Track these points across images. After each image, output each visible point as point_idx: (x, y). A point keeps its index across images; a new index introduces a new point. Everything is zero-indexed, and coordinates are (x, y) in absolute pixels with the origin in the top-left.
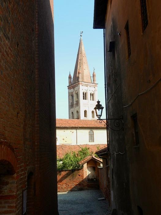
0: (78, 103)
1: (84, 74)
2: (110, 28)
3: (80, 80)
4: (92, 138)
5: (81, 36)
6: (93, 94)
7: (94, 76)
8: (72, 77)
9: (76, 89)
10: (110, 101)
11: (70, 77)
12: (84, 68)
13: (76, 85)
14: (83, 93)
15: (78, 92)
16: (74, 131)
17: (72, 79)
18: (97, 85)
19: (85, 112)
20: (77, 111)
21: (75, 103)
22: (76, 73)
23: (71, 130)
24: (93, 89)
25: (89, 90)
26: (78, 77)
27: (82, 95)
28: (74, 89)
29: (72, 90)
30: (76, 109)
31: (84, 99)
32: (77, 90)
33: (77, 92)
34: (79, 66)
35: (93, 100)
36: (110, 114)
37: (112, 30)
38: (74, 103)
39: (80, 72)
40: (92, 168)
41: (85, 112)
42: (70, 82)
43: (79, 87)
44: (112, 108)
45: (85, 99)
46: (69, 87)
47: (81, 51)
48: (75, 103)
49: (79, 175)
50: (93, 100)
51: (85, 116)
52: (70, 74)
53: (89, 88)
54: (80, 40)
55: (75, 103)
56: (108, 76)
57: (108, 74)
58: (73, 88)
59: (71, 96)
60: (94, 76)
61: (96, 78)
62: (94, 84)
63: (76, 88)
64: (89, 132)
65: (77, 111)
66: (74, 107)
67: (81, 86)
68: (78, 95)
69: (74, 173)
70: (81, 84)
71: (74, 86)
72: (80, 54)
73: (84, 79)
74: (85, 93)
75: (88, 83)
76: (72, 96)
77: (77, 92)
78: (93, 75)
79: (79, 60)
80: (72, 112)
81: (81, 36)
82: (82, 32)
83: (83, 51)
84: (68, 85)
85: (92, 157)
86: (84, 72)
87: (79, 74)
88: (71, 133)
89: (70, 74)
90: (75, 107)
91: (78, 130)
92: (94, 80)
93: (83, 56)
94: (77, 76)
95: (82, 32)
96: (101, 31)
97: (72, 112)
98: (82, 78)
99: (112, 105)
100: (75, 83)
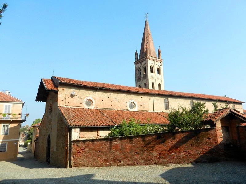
0: (146, 76)
1: (151, 50)
3: (148, 54)
4: (167, 106)
5: (146, 17)
7: (159, 52)
8: (139, 54)
9: (143, 63)
11: (136, 54)
12: (151, 45)
13: (143, 60)
14: (151, 67)
15: (145, 66)
16: (151, 98)
17: (138, 56)
18: (162, 60)
19: (153, 84)
20: (145, 84)
21: (142, 76)
22: (143, 49)
23: (148, 97)
24: (159, 64)
25: (157, 64)
26: (146, 53)
27: (150, 69)
28: (141, 64)
29: (139, 65)
30: (144, 81)
31: (151, 72)
34: (145, 43)
39: (148, 47)
40: (224, 128)
41: (153, 84)
42: (137, 58)
43: (146, 61)
46: (136, 63)
47: (147, 30)
48: (143, 76)
49: (209, 139)
50: (159, 74)
52: (136, 51)
53: (156, 63)
55: (142, 76)
58: (141, 63)
59: (138, 70)
60: (159, 52)
61: (161, 54)
62: (159, 59)
63: (144, 62)
64: (165, 100)
65: (145, 84)
66: (142, 80)
67: (148, 60)
68: (145, 69)
69: (199, 135)
70: (149, 58)
72: (146, 32)
76: (139, 71)
78: (159, 51)
79: (145, 38)
81: (146, 17)
82: (148, 14)
83: (149, 30)
85: (231, 111)
86: (151, 48)
87: (146, 49)
88: (148, 99)
89: (136, 51)
90: (143, 80)
91: (155, 97)
92: (159, 56)
93: (149, 34)
94: (145, 51)
95: (148, 14)
98: (149, 53)
100: (143, 58)
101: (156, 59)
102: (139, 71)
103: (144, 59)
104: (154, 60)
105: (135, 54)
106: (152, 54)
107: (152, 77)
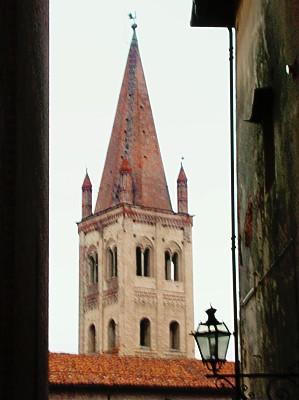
2: (253, 34)
6: (175, 255)
10: (253, 303)
11: (87, 188)
15: (116, 248)
31: (139, 273)
32: (114, 238)
33: (112, 247)
35: (176, 279)
36: (251, 348)
37: (261, 46)
38: (101, 291)
42: (87, 206)
44: (258, 327)
45: (146, 275)
51: (143, 343)
53: (161, 231)
54: (134, 46)
56: (245, 206)
57: (244, 199)
58: (100, 228)
62: (176, 217)
66: (101, 306)
71: (101, 221)
73: (141, 197)
74: (143, 251)
75: (156, 210)
76: (94, 261)
77: (112, 247)
80: (93, 328)
84: (79, 220)
90: (104, 306)
96: (220, 35)
97: (93, 328)
99: (259, 315)
100: (106, 211)
101: (165, 216)
102: (94, 261)
103: (113, 217)
104: (152, 222)
105: (84, 189)
106: (145, 194)
107: (139, 293)
